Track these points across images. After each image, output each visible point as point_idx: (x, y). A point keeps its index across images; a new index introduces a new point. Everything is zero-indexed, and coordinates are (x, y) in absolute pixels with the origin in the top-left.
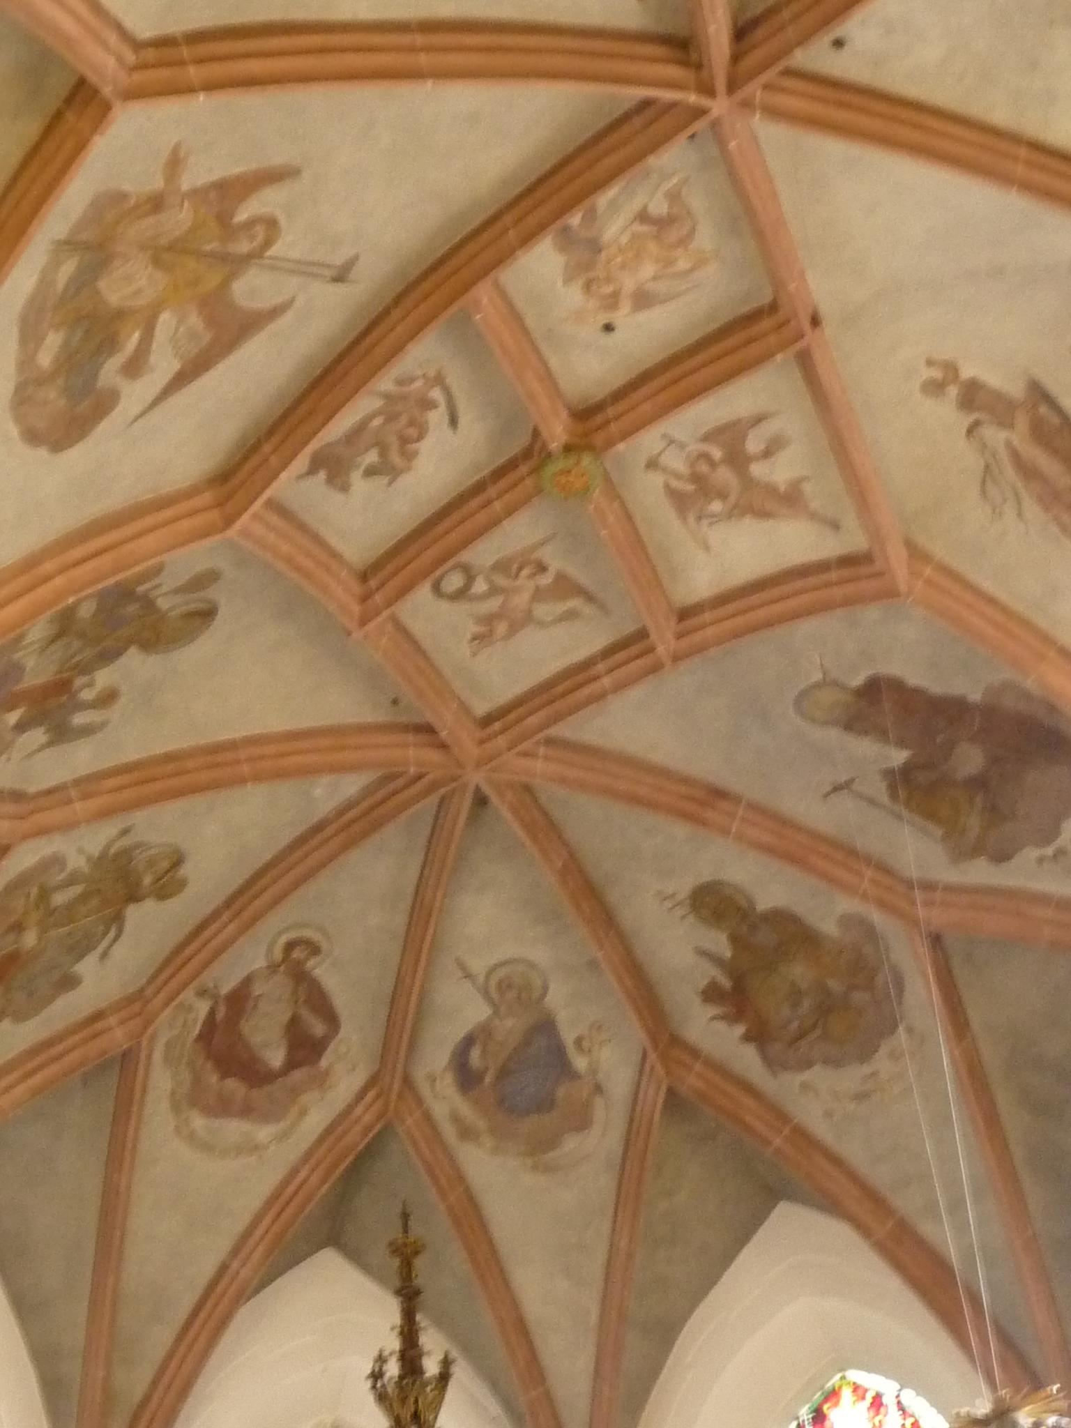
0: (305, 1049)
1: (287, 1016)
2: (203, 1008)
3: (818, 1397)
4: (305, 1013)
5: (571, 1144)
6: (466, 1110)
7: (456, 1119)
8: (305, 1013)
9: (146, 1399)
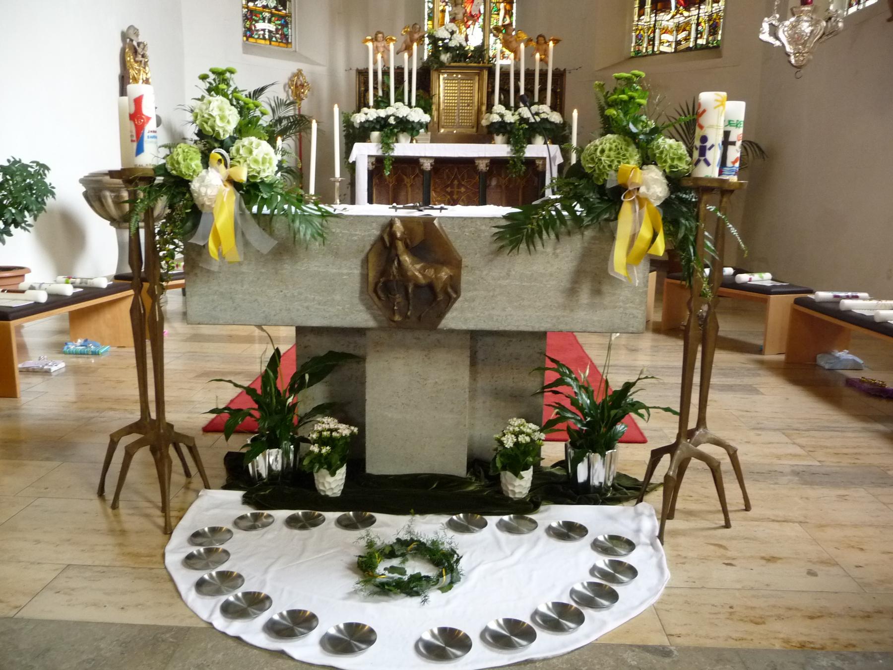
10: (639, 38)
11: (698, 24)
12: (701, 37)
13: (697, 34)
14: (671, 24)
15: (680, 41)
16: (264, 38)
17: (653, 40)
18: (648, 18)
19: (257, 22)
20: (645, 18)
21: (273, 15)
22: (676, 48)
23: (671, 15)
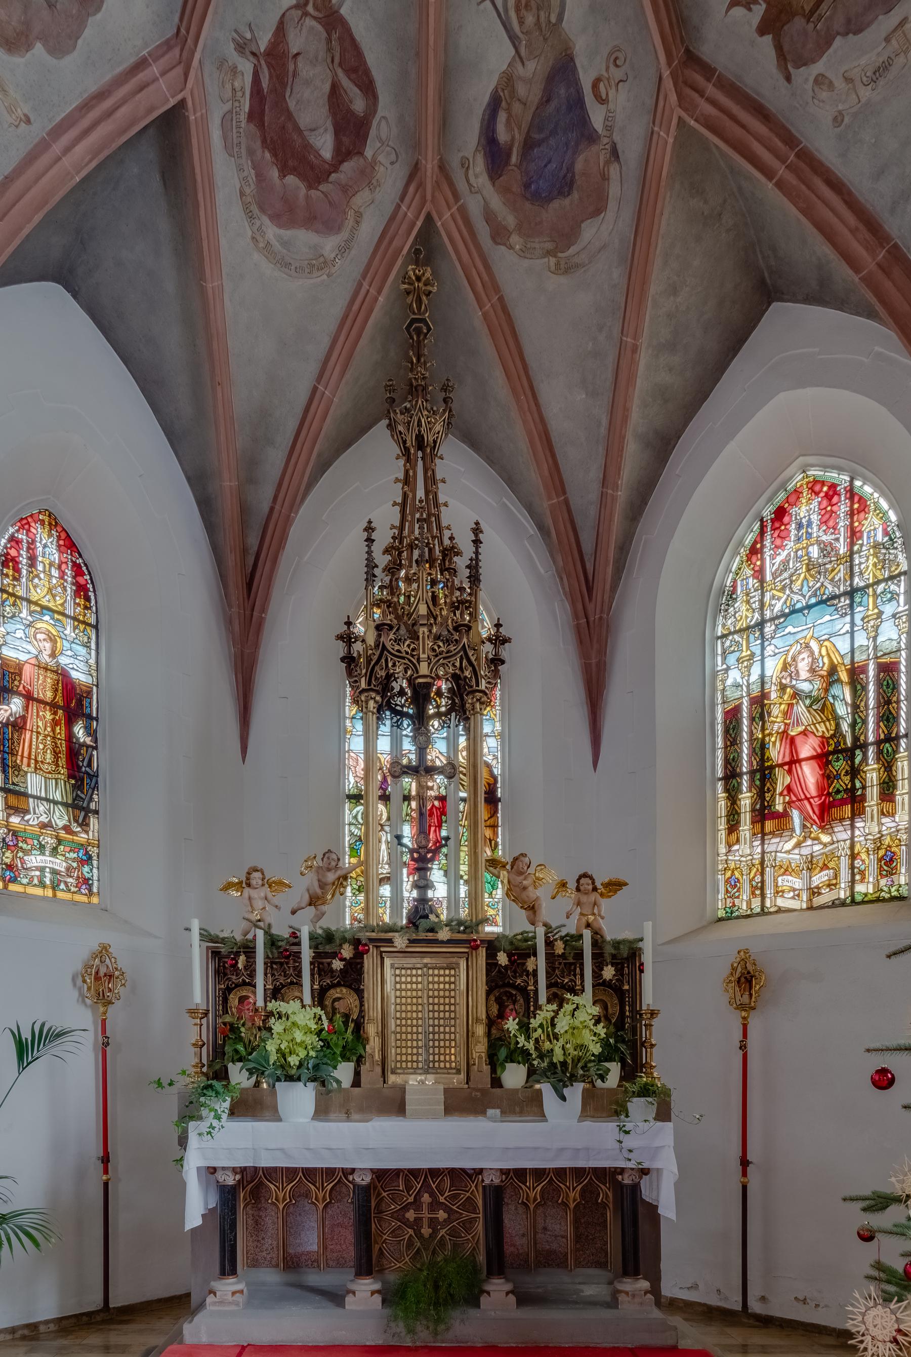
0: (352, 131)
1: (327, 87)
2: (246, 67)
3: (782, 496)
4: (345, 82)
5: (590, 231)
6: (496, 202)
7: (489, 216)
8: (345, 82)
9: (272, 509)
10: (733, 884)
11: (853, 856)
12: (862, 880)
13: (853, 875)
14: (795, 857)
15: (818, 887)
16: (42, 884)
17: (762, 889)
18: (747, 848)
19: (26, 852)
20: (743, 849)
21: (60, 841)
22: (810, 900)
23: (794, 841)
